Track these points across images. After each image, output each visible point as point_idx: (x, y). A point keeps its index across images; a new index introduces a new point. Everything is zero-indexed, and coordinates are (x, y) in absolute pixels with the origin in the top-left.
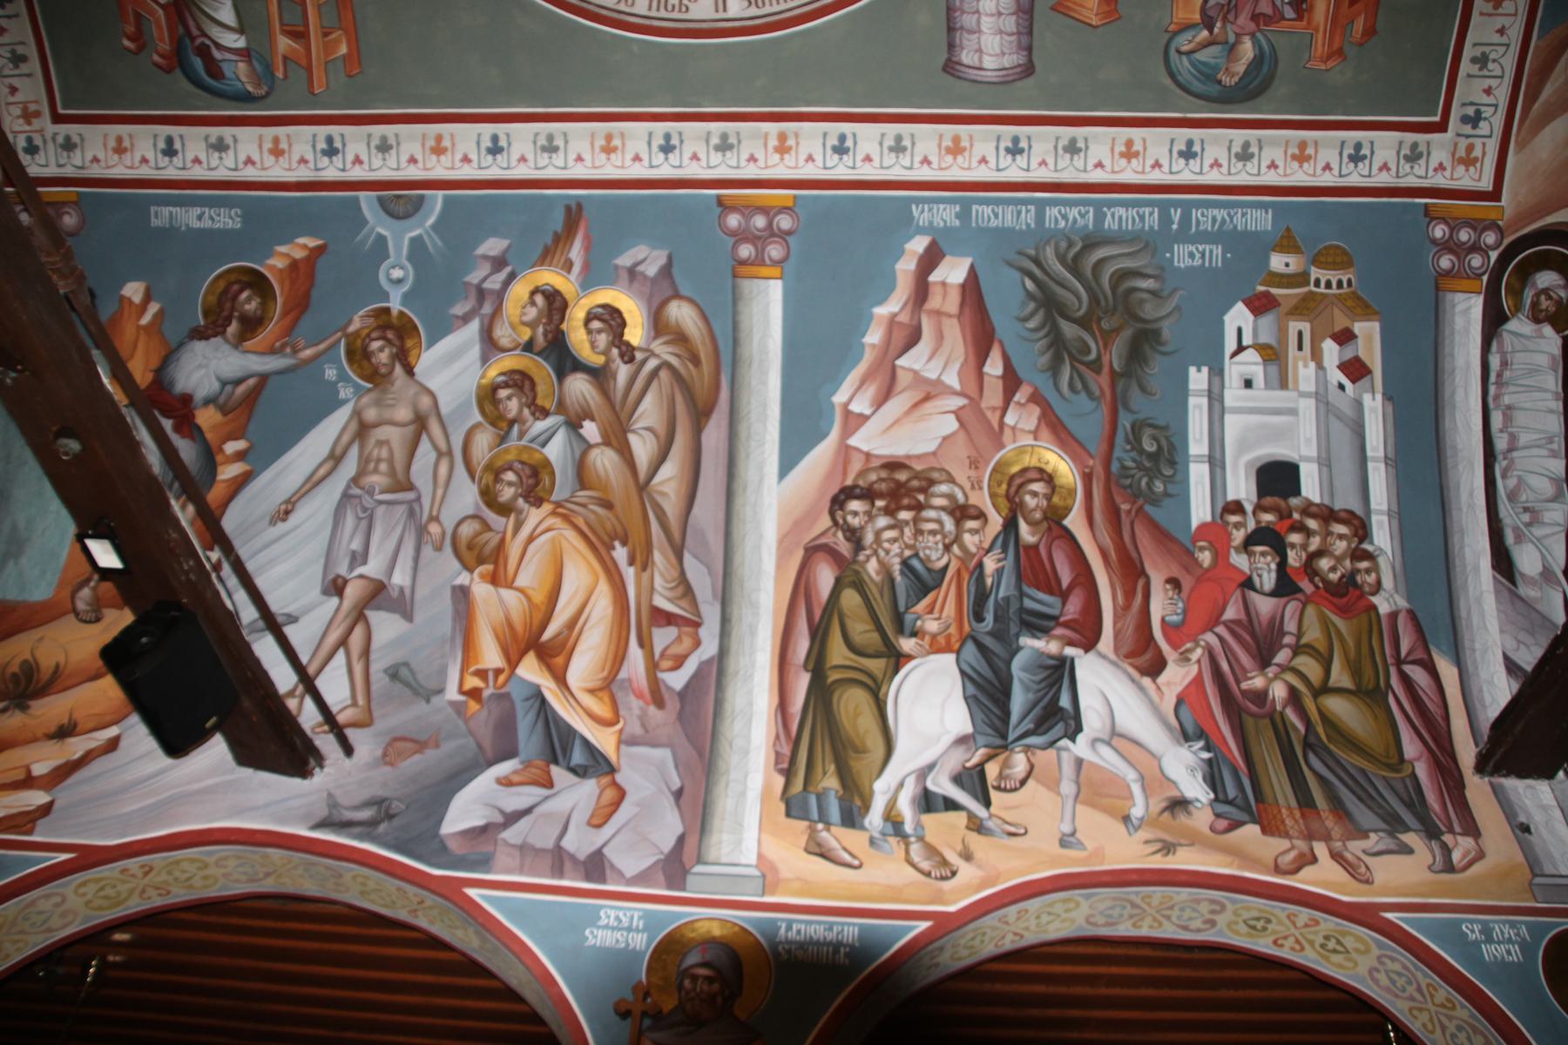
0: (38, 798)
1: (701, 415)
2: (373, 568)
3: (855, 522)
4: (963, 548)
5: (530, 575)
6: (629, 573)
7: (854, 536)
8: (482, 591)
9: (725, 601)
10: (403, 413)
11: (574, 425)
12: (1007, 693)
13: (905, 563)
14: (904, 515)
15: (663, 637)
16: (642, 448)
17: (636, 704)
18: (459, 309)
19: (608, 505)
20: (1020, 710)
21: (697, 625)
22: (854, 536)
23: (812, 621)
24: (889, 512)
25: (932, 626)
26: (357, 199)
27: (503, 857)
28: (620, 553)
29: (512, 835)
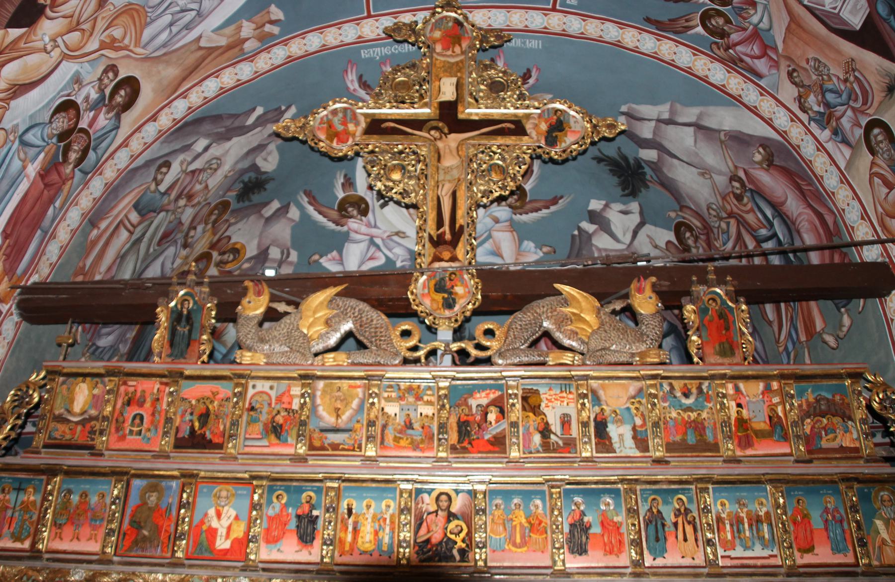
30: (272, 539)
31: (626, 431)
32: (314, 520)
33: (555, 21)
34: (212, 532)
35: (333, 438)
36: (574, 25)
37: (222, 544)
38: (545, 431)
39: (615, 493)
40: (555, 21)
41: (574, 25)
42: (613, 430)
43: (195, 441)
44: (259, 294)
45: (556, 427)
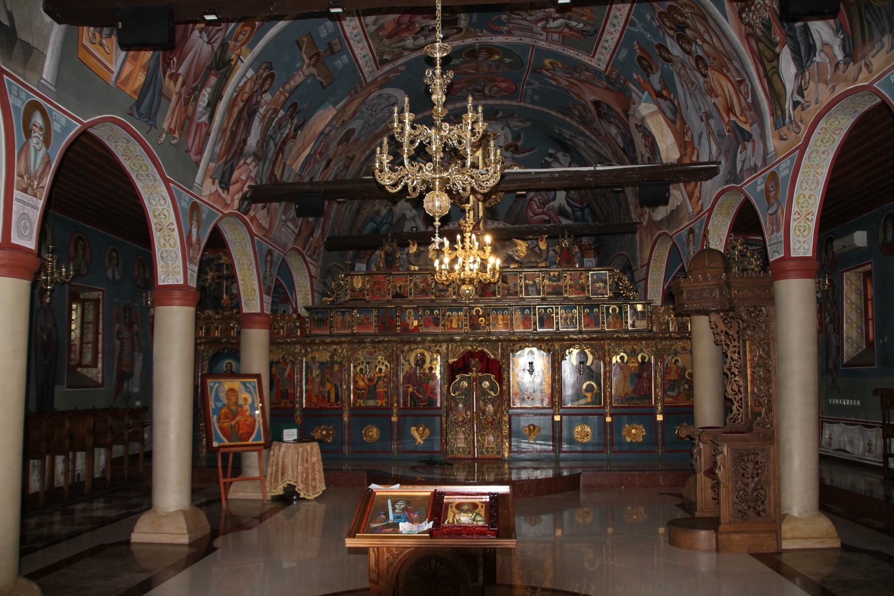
0: (700, 202)
1: (705, 19)
2: (703, 111)
3: (747, 20)
4: (769, 7)
5: (719, 92)
6: (728, 74)
7: (748, 24)
8: (716, 100)
9: (744, 69)
10: (680, 65)
11: (696, 43)
12: (800, 50)
13: (763, 24)
14: (753, 8)
15: (742, 88)
16: (707, 37)
17: (747, 113)
18: (662, 34)
19: (715, 59)
20: (804, 53)
21: (744, 80)
22: (748, 24)
23: (759, 58)
24: (750, 10)
25: (778, 39)
26: (628, 30)
27: (745, 176)
28: (725, 71)
29: (745, 168)
30: (426, 326)
31: (534, 289)
32: (438, 319)
33: (522, 104)
34: (408, 324)
35: (443, 294)
36: (530, 106)
37: (411, 328)
38: (508, 289)
39: (530, 309)
40: (522, 104)
41: (530, 106)
42: (530, 289)
43: (397, 295)
44: (414, 245)
45: (512, 288)
